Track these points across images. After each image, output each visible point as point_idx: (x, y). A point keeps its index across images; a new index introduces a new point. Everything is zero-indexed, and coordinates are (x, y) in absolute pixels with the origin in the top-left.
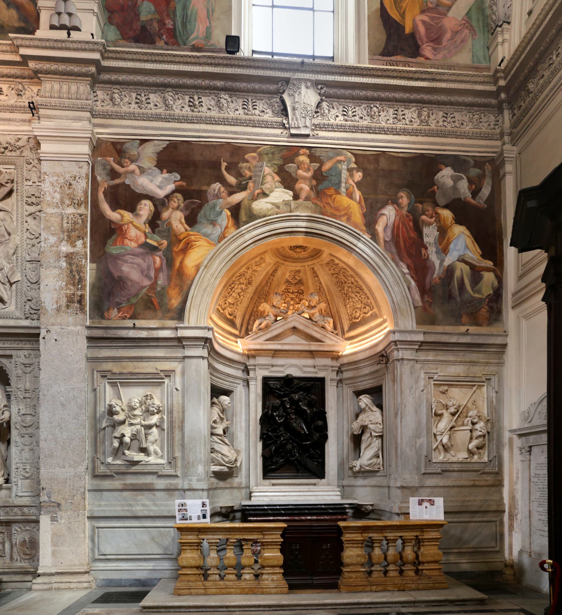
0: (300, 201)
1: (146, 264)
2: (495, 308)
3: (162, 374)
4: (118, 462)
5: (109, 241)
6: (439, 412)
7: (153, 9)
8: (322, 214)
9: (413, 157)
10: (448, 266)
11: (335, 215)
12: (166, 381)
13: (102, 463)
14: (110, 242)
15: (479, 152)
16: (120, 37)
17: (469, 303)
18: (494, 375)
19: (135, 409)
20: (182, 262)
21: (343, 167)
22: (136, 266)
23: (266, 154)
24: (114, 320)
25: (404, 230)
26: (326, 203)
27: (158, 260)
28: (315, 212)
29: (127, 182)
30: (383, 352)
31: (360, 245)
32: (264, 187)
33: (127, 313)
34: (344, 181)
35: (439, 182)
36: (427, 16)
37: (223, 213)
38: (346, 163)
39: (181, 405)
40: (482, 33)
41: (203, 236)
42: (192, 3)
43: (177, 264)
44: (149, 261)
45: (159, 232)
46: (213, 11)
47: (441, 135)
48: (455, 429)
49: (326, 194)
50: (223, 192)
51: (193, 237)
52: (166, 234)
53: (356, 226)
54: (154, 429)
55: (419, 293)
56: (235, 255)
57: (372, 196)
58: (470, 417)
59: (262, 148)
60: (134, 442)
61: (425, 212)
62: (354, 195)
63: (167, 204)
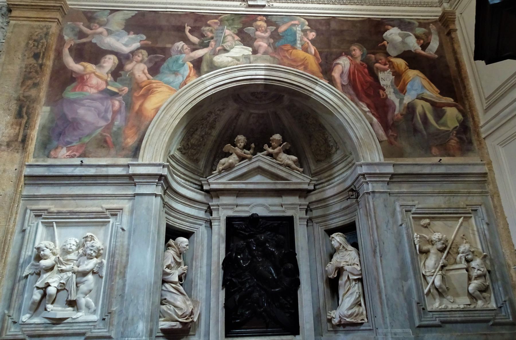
0: (259, 55)
1: (104, 108)
2: (465, 139)
3: (108, 213)
4: (36, 320)
5: (68, 88)
6: (425, 248)
8: (280, 64)
9: (361, 21)
10: (408, 103)
12: (111, 220)
13: (15, 323)
14: (69, 88)
15: (422, 16)
17: (437, 135)
18: (480, 205)
19: (69, 253)
20: (141, 106)
21: (298, 28)
22: (93, 109)
23: (227, 20)
24: (61, 158)
25: (360, 75)
27: (117, 103)
28: (274, 63)
29: (94, 41)
30: (352, 187)
31: (318, 88)
32: (224, 45)
33: (77, 152)
34: (299, 39)
37: (186, 65)
38: (300, 26)
39: (126, 247)
41: (165, 83)
43: (137, 107)
45: (121, 80)
47: (384, 4)
48: (447, 268)
49: (282, 49)
50: (186, 49)
53: (313, 74)
54: (90, 277)
55: (382, 128)
56: (195, 99)
57: (326, 50)
58: (463, 253)
59: (223, 16)
60: (61, 293)
62: (309, 49)
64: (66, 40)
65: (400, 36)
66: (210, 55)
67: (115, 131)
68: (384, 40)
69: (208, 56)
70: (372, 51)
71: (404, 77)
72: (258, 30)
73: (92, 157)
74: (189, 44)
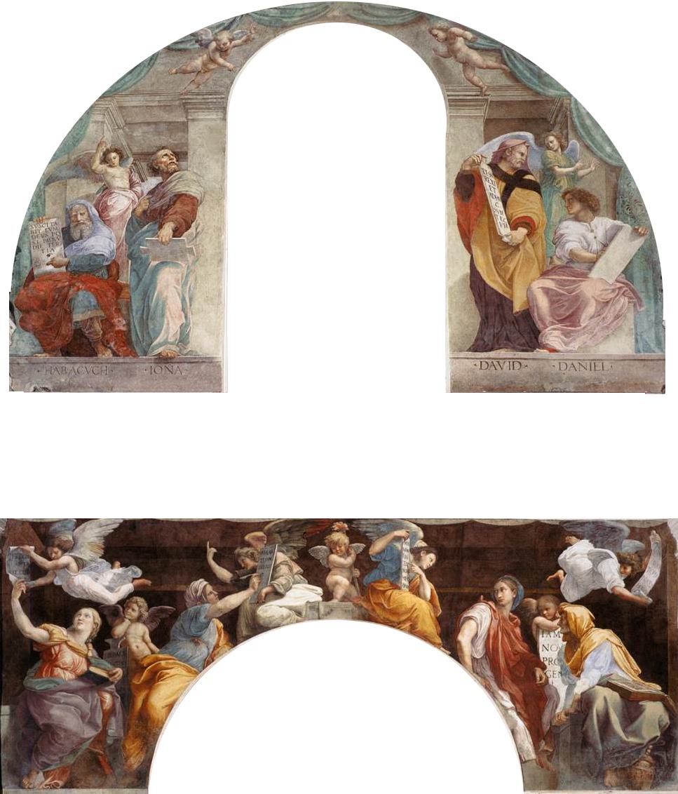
0: (335, 601)
5: (30, 671)
7: (94, 301)
11: (391, 622)
14: (31, 672)
16: (39, 348)
21: (404, 546)
22: (72, 707)
23: (280, 532)
26: (375, 603)
27: (108, 697)
29: (58, 582)
33: (59, 780)
34: (406, 568)
35: (566, 564)
36: (552, 279)
37: (211, 624)
38: (408, 540)
40: (653, 301)
42: (158, 288)
43: (139, 703)
44: (93, 701)
45: (110, 656)
46: (191, 299)
50: (211, 593)
51: (163, 663)
52: (121, 659)
55: (531, 740)
57: (453, 590)
61: (542, 611)
62: (421, 590)
63: (122, 613)
64: (13, 582)
65: (590, 560)
66: (251, 604)
67: (110, 746)
68: (559, 568)
69: (248, 606)
70: (535, 591)
71: (585, 643)
72: (334, 551)
73: (82, 787)
74: (215, 584)
